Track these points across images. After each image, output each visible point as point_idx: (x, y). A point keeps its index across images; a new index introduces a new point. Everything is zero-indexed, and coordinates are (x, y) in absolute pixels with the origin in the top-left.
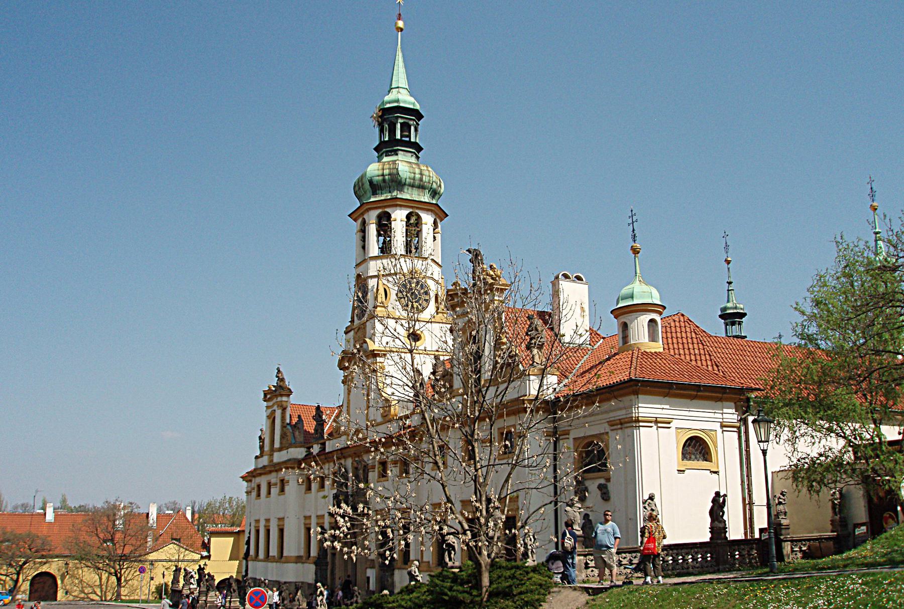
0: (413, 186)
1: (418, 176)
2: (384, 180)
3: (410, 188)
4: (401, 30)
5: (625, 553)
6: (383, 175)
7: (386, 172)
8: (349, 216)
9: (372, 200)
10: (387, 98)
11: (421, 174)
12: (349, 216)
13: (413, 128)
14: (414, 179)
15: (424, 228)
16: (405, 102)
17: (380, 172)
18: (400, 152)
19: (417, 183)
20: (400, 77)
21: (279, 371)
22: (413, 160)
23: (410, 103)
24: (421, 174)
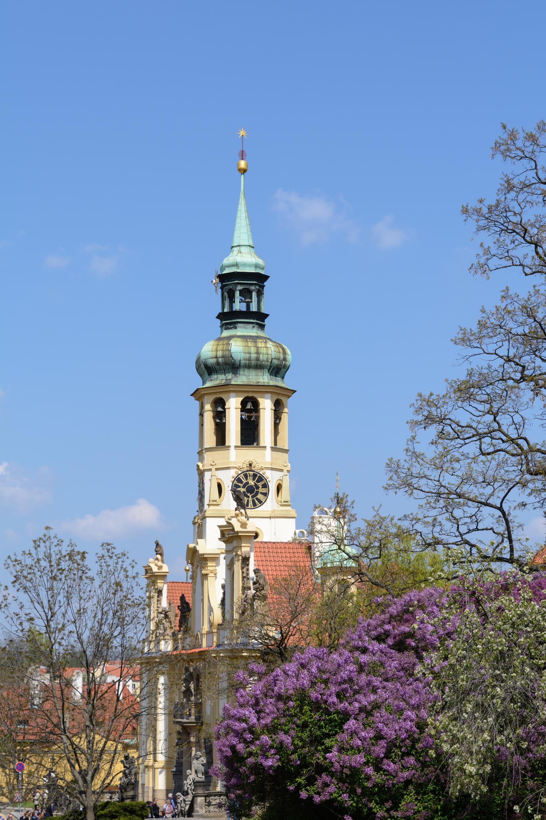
0: (249, 367)
1: (254, 356)
2: (218, 363)
3: (246, 370)
4: (244, 171)
5: (215, 796)
6: (216, 357)
7: (220, 354)
8: (191, 395)
9: (208, 384)
10: (226, 262)
11: (258, 353)
12: (191, 395)
13: (254, 295)
14: (249, 360)
15: (261, 411)
16: (245, 265)
17: (214, 354)
18: (239, 325)
19: (253, 363)
20: (242, 233)
21: (157, 544)
22: (253, 332)
23: (250, 265)
24: (258, 353)
